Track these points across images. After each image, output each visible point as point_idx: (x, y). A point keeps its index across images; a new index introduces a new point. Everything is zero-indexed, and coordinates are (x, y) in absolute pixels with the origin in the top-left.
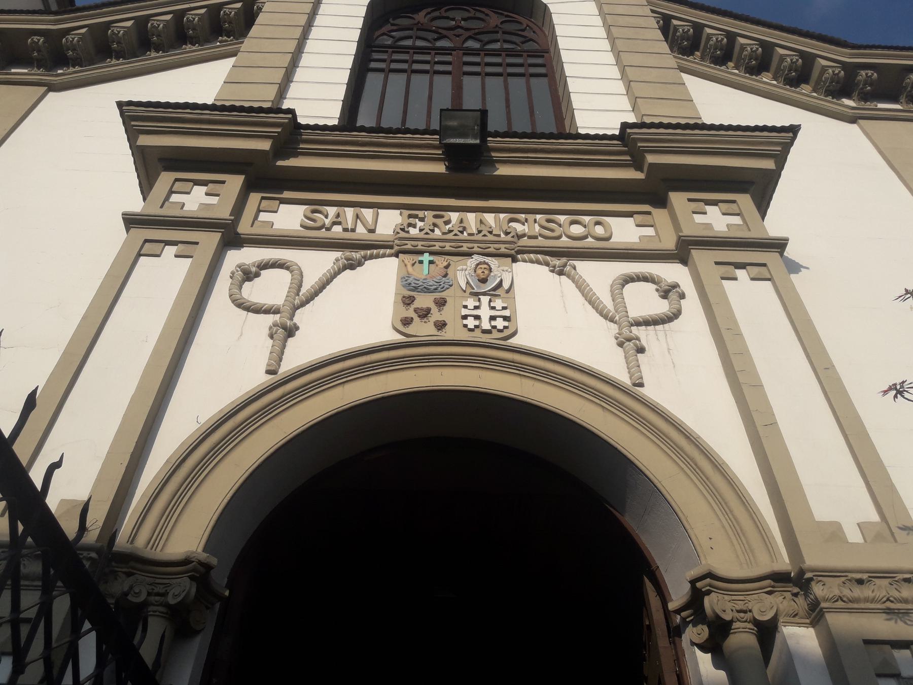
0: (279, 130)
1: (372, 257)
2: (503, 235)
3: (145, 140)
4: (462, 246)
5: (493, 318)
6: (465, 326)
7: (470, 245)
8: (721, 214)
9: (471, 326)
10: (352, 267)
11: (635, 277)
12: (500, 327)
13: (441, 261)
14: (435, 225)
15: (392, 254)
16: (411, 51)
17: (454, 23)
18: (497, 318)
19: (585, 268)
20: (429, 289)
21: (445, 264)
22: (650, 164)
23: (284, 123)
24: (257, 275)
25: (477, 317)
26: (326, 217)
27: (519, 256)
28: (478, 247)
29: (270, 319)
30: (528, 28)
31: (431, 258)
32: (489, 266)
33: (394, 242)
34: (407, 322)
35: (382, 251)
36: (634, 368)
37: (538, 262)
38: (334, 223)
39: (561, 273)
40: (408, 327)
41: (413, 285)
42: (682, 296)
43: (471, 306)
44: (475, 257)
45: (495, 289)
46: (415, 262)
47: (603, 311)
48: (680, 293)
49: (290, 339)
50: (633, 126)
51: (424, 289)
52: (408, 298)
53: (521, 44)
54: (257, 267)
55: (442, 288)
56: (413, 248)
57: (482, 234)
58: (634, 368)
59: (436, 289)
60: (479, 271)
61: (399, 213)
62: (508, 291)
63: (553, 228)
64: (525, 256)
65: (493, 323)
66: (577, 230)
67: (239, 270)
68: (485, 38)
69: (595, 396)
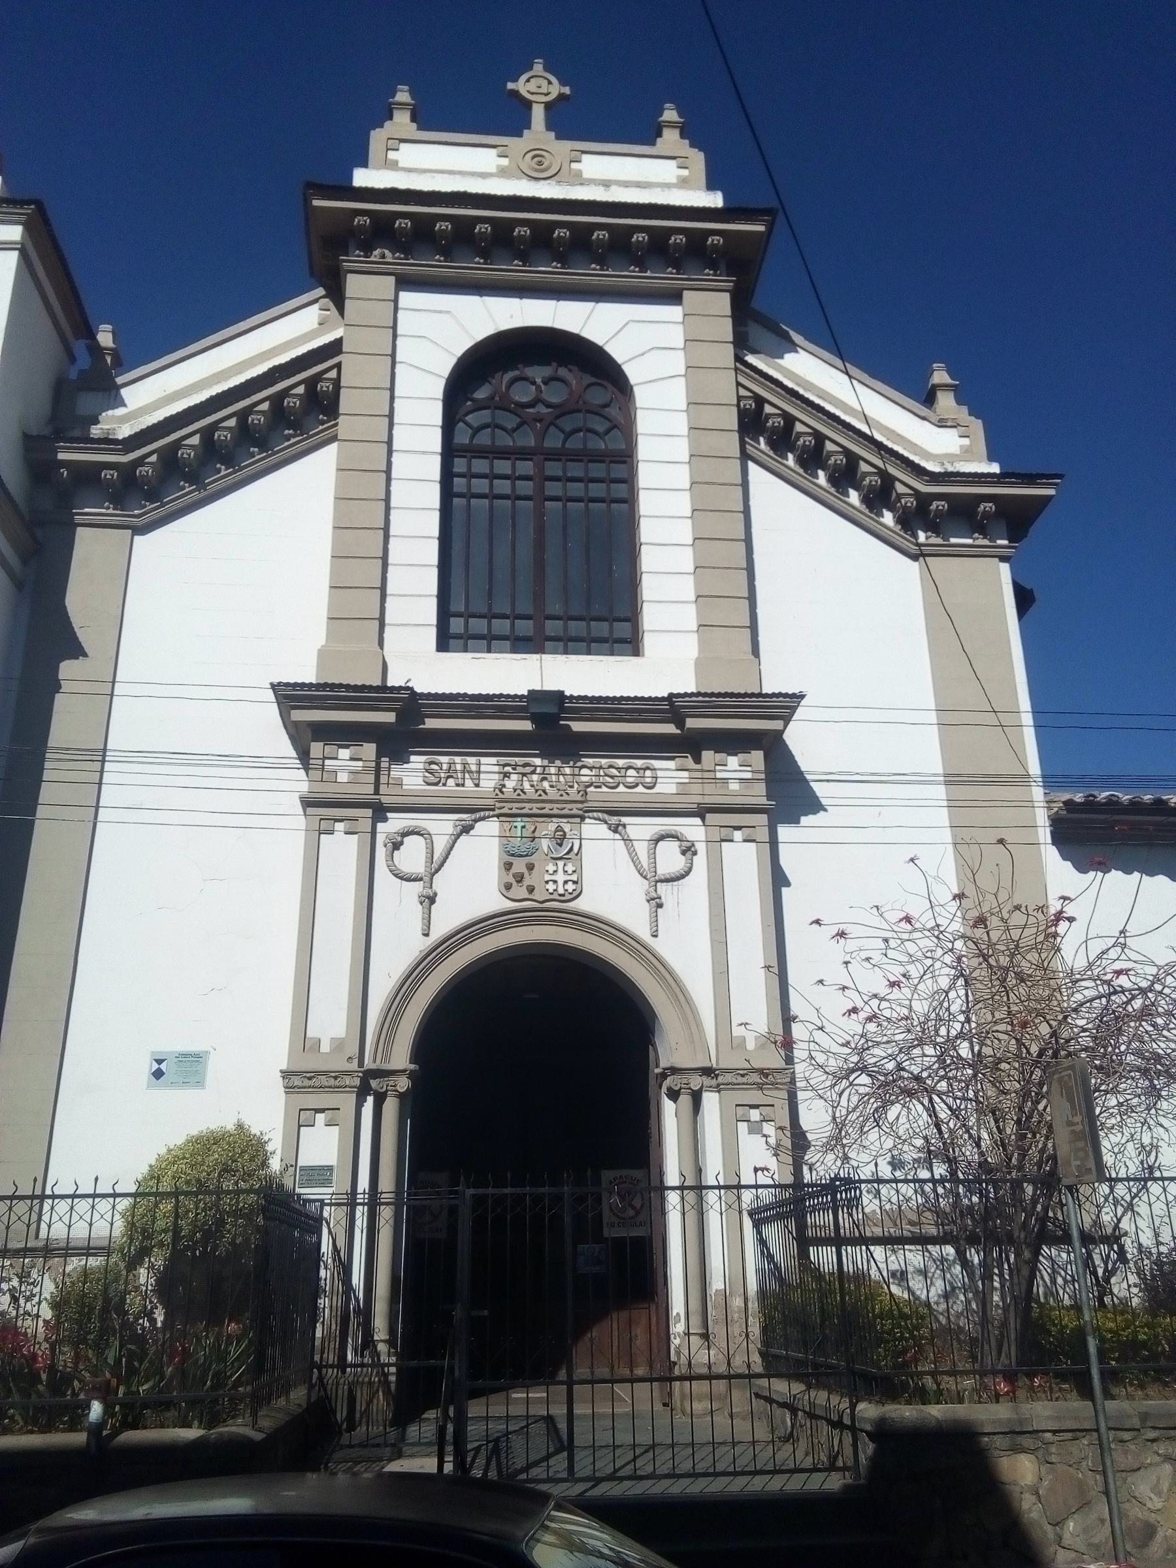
3: (299, 715)
5: (566, 882)
9: (551, 891)
12: (570, 891)
21: (533, 828)
24: (401, 843)
25: (555, 882)
27: (586, 814)
34: (508, 887)
35: (487, 813)
36: (655, 921)
37: (599, 819)
39: (616, 831)
42: (695, 853)
43: (551, 872)
44: (554, 820)
45: (568, 853)
49: (433, 907)
50: (679, 695)
58: (655, 921)
62: (577, 855)
64: (590, 814)
65: (566, 887)
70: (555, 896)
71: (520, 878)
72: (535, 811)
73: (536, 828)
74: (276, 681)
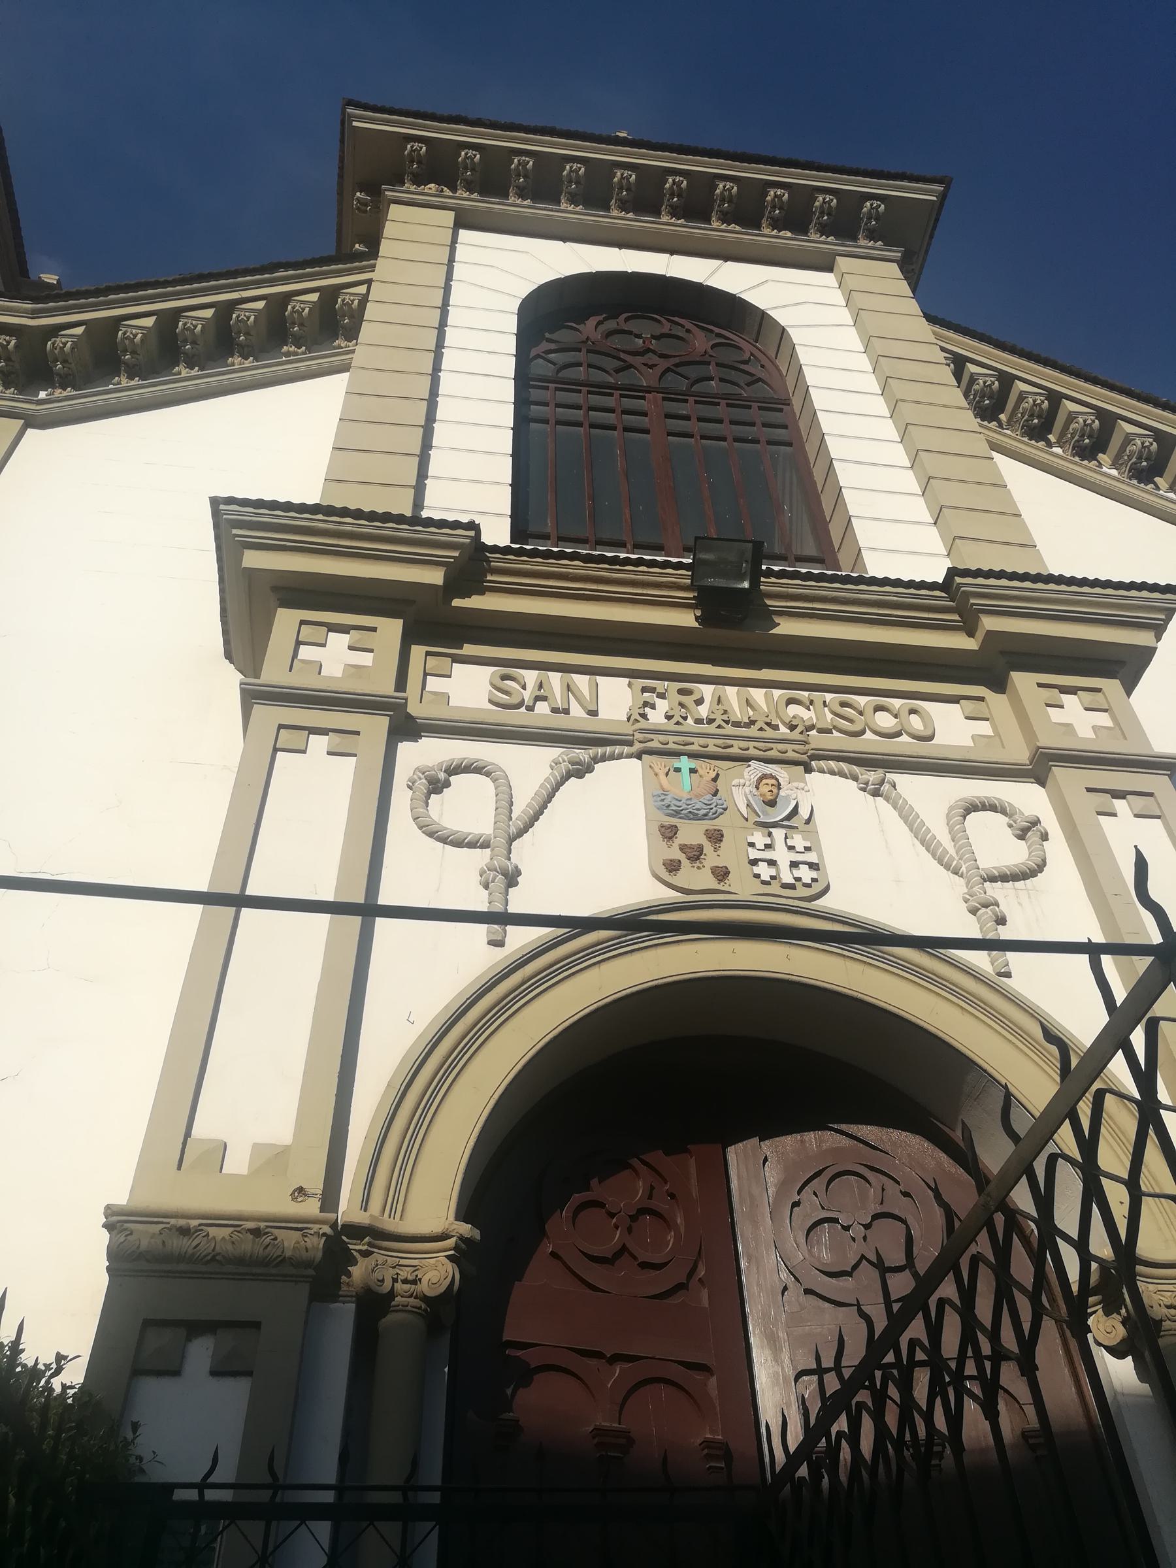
0: (456, 554)
1: (604, 758)
2: (783, 729)
4: (732, 746)
5: (794, 865)
6: (757, 876)
7: (743, 744)
8: (1082, 708)
10: (580, 775)
11: (979, 804)
13: (707, 769)
14: (681, 705)
15: (633, 754)
16: (585, 389)
17: (641, 341)
18: (800, 865)
19: (908, 784)
20: (697, 814)
21: (713, 775)
22: (989, 633)
23: (463, 544)
24: (447, 784)
25: (772, 863)
26: (524, 687)
28: (755, 747)
29: (481, 857)
30: (752, 357)
31: (693, 764)
32: (777, 780)
33: (633, 735)
34: (673, 867)
35: (618, 749)
37: (842, 775)
38: (538, 699)
39: (876, 793)
40: (676, 875)
41: (675, 808)
44: (753, 764)
45: (789, 817)
46: (669, 770)
47: (945, 857)
48: (1042, 833)
50: (966, 573)
51: (689, 815)
52: (669, 828)
53: (746, 387)
54: (444, 771)
55: (714, 814)
56: (663, 746)
57: (758, 725)
59: (706, 815)
60: (764, 789)
61: (627, 683)
62: (808, 822)
63: (852, 717)
64: (822, 763)
65: (797, 873)
66: (885, 721)
67: (422, 776)
68: (693, 372)
69: (951, 992)
70: (775, 888)
71: (695, 854)
72: (712, 749)
73: (718, 775)
74: (225, 494)
